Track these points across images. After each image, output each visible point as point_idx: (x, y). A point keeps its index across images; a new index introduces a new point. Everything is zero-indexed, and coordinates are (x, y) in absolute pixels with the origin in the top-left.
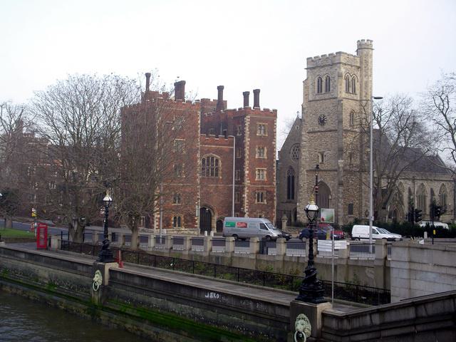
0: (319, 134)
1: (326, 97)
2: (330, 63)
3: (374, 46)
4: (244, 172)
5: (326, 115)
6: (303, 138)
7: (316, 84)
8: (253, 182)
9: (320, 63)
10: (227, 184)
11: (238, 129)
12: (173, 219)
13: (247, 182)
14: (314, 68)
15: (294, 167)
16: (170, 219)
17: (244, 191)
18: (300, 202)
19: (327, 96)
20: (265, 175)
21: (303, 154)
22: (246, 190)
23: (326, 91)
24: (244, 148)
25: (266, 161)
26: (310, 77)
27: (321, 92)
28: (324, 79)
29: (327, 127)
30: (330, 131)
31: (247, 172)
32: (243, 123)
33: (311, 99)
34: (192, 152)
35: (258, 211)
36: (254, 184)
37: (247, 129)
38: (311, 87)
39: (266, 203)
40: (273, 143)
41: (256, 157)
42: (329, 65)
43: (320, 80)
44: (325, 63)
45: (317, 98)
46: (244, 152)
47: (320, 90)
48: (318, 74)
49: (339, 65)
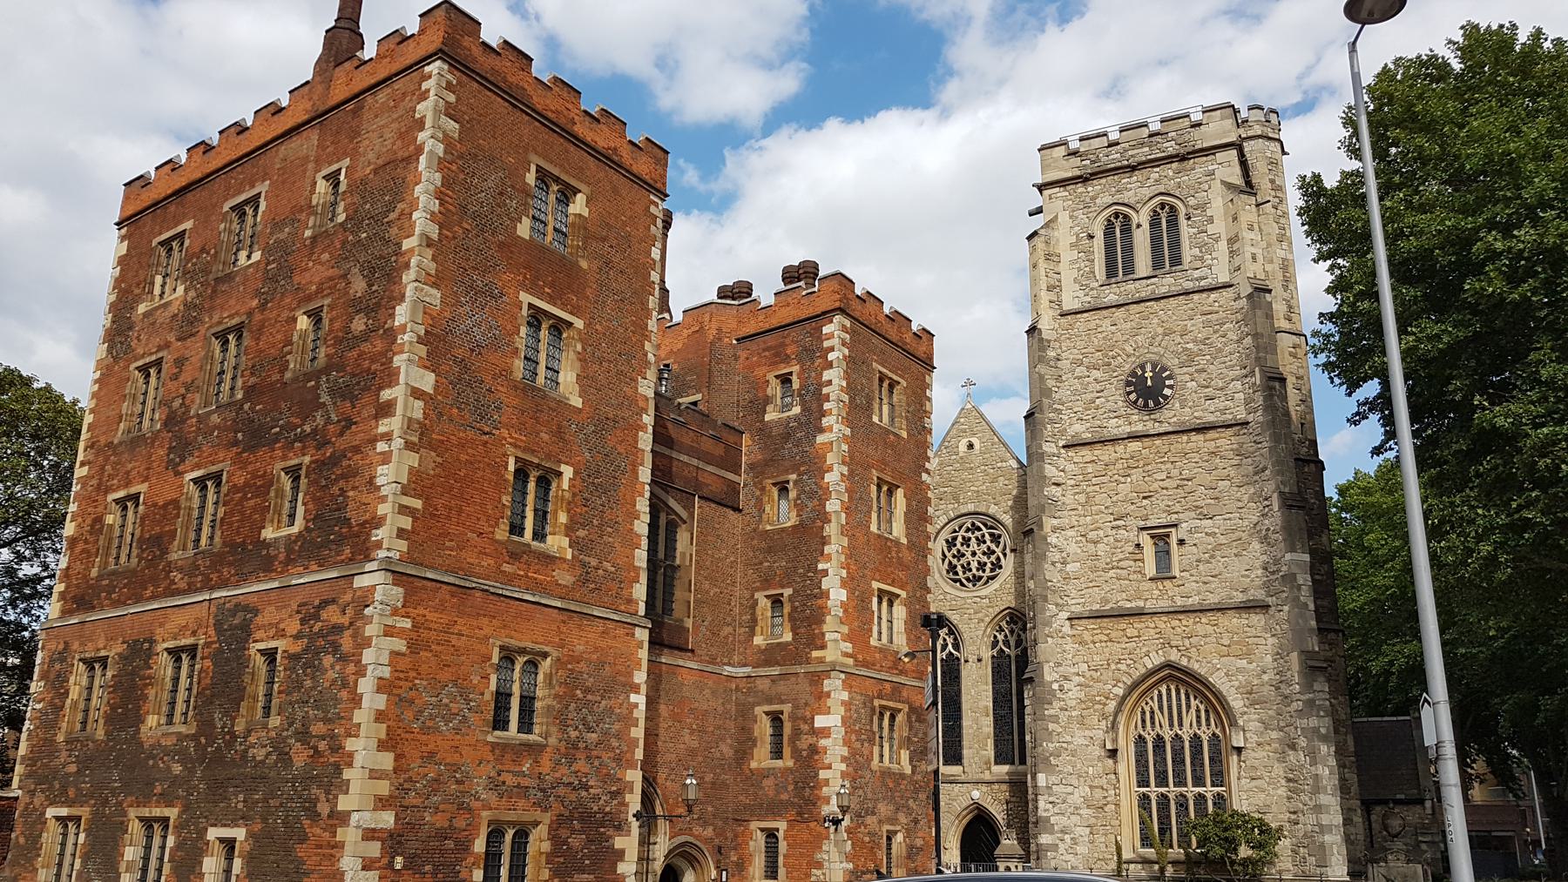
0: (1135, 446)
1: (1163, 290)
2: (1171, 147)
3: (1489, 19)
4: (826, 595)
5: (1172, 362)
6: (1050, 471)
7: (1099, 243)
8: (864, 655)
9: (1114, 157)
10: (713, 661)
11: (774, 388)
12: (479, 846)
13: (836, 646)
14: (1084, 179)
15: (954, 617)
16: (464, 847)
17: (822, 696)
18: (1051, 769)
19: (1166, 284)
20: (899, 625)
21: (1052, 539)
22: (836, 688)
23: (1157, 263)
24: (824, 470)
25: (907, 556)
26: (1064, 218)
27: (1129, 268)
28: (1142, 218)
29: (1172, 415)
30: (1202, 429)
31: (837, 595)
32: (814, 354)
33: (1069, 303)
34: (609, 422)
35: (884, 809)
36: (866, 664)
37: (835, 378)
38: (1068, 255)
39: (908, 770)
40: (924, 476)
41: (874, 528)
42: (1169, 159)
43: (1119, 226)
44: (1143, 153)
45: (1111, 296)
46: (822, 495)
47: (1118, 263)
48: (1110, 200)
49: (1220, 156)
